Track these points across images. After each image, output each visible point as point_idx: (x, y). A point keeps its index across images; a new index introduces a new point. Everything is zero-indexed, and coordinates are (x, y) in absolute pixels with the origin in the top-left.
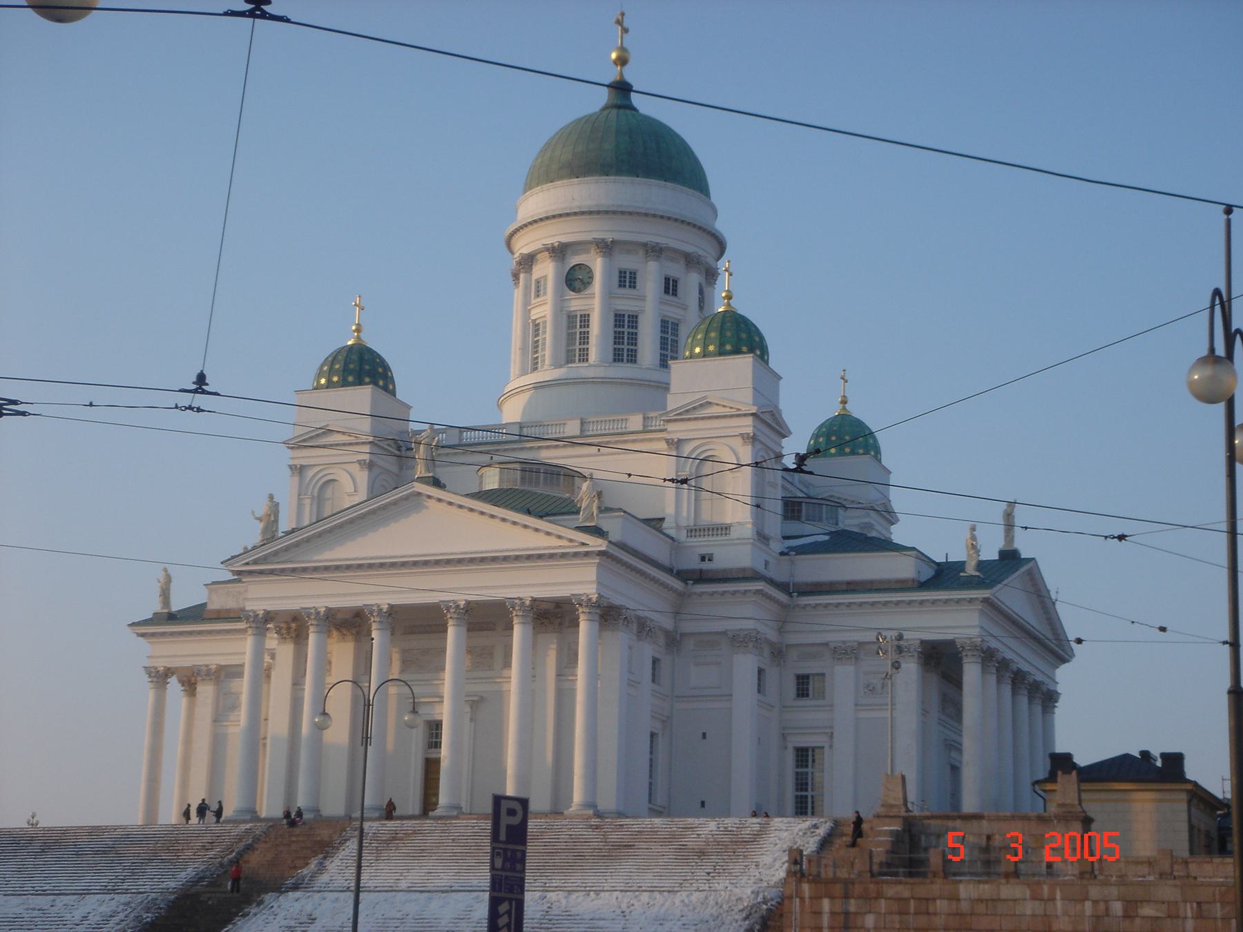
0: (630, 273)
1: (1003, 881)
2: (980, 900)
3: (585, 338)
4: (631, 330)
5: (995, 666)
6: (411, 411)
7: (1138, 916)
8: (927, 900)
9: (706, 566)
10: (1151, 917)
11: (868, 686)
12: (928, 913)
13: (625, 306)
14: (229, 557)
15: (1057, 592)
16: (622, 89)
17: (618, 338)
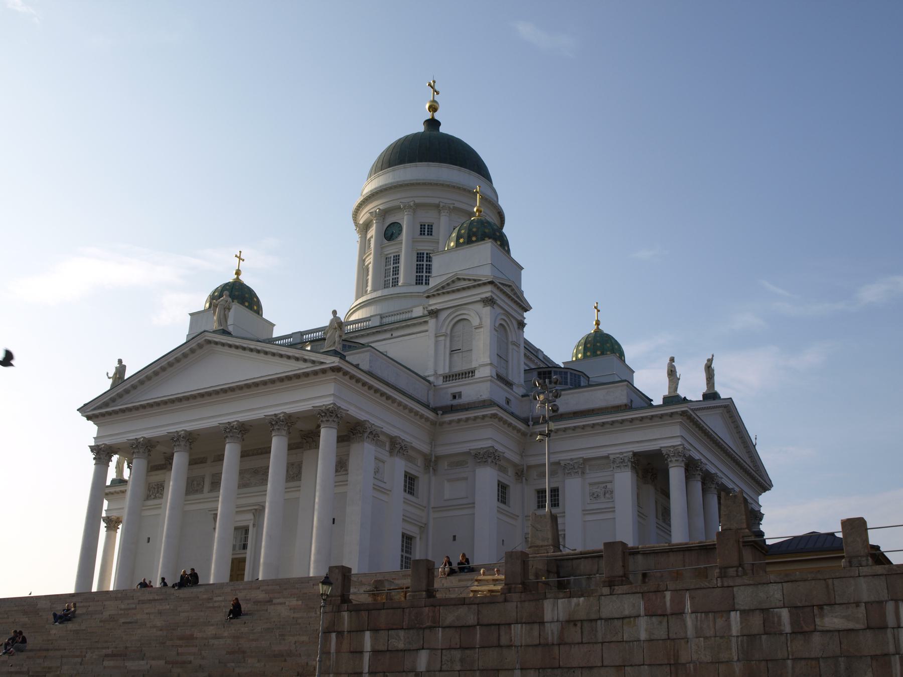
0: (428, 225)
1: (606, 590)
2: (571, 622)
3: (396, 271)
4: (428, 263)
5: (699, 474)
6: (274, 327)
7: (815, 631)
8: (499, 625)
9: (455, 402)
10: (839, 631)
11: (593, 494)
12: (499, 646)
13: (425, 248)
14: (83, 405)
15: (756, 439)
16: (433, 124)
17: (419, 269)
